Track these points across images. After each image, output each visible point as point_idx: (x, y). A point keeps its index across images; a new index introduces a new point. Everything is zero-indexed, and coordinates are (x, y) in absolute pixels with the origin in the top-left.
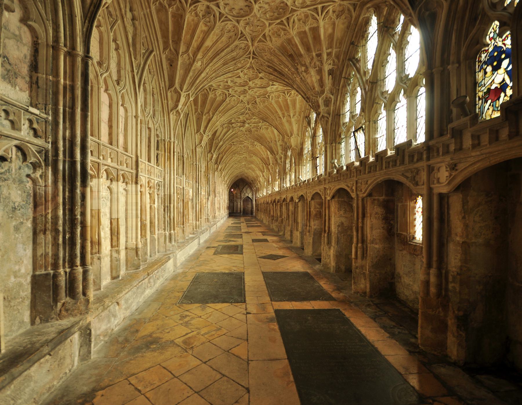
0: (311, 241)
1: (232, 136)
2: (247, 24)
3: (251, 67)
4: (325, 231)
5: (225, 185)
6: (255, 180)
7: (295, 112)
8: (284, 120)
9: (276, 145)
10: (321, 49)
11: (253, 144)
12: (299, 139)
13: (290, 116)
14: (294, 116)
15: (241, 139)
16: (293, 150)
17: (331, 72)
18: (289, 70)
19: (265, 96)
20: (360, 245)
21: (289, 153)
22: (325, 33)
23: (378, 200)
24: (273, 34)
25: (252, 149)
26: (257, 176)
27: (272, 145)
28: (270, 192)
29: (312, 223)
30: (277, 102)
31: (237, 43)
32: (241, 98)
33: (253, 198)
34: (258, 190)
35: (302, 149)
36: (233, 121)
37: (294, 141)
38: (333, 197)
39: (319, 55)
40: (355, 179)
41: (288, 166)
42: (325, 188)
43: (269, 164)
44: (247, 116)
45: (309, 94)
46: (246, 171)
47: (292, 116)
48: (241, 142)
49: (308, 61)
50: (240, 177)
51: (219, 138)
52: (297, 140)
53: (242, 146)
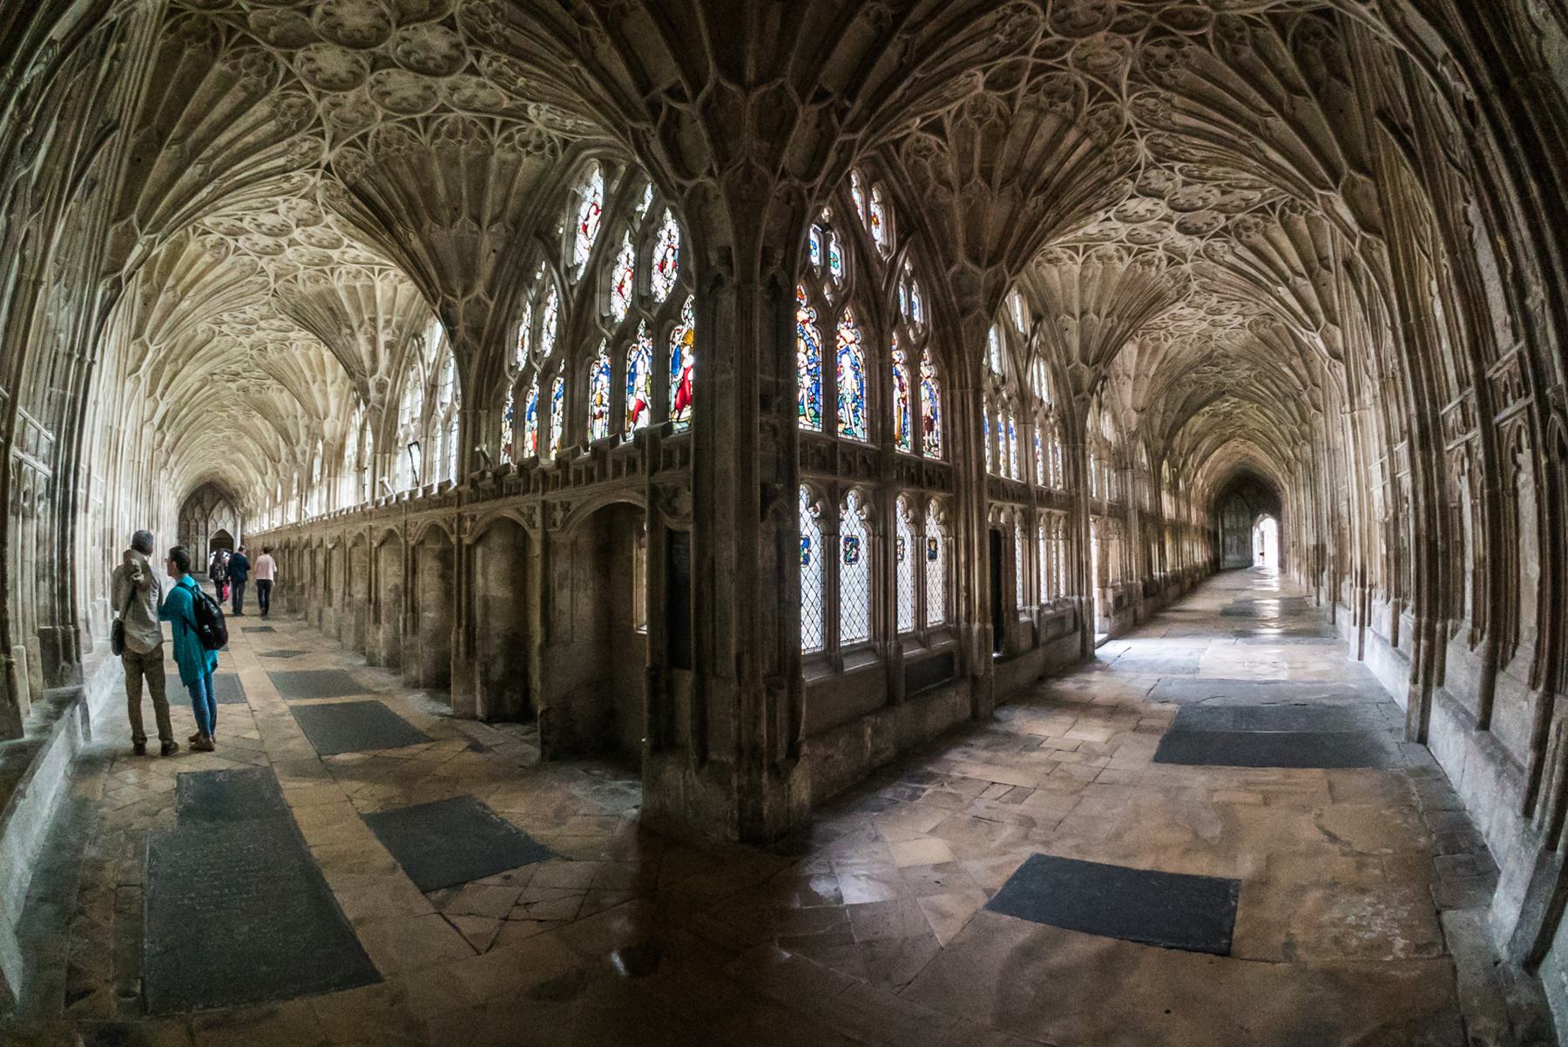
0: (353, 622)
1: (209, 397)
4: (370, 600)
5: (174, 500)
7: (336, 378)
8: (315, 388)
9: (296, 425)
12: (339, 424)
13: (325, 382)
14: (333, 382)
16: (326, 445)
18: (328, 326)
19: (284, 344)
20: (409, 614)
21: (320, 445)
22: (383, 296)
23: (432, 550)
24: (309, 278)
27: (289, 423)
28: (277, 524)
29: (354, 590)
33: (235, 534)
34: (248, 515)
35: (342, 446)
37: (328, 428)
38: (382, 544)
39: (373, 320)
40: (403, 518)
41: (316, 471)
42: (371, 527)
45: (355, 367)
46: (225, 466)
47: (329, 382)
49: (355, 325)
50: (208, 480)
52: (336, 426)
53: (224, 414)
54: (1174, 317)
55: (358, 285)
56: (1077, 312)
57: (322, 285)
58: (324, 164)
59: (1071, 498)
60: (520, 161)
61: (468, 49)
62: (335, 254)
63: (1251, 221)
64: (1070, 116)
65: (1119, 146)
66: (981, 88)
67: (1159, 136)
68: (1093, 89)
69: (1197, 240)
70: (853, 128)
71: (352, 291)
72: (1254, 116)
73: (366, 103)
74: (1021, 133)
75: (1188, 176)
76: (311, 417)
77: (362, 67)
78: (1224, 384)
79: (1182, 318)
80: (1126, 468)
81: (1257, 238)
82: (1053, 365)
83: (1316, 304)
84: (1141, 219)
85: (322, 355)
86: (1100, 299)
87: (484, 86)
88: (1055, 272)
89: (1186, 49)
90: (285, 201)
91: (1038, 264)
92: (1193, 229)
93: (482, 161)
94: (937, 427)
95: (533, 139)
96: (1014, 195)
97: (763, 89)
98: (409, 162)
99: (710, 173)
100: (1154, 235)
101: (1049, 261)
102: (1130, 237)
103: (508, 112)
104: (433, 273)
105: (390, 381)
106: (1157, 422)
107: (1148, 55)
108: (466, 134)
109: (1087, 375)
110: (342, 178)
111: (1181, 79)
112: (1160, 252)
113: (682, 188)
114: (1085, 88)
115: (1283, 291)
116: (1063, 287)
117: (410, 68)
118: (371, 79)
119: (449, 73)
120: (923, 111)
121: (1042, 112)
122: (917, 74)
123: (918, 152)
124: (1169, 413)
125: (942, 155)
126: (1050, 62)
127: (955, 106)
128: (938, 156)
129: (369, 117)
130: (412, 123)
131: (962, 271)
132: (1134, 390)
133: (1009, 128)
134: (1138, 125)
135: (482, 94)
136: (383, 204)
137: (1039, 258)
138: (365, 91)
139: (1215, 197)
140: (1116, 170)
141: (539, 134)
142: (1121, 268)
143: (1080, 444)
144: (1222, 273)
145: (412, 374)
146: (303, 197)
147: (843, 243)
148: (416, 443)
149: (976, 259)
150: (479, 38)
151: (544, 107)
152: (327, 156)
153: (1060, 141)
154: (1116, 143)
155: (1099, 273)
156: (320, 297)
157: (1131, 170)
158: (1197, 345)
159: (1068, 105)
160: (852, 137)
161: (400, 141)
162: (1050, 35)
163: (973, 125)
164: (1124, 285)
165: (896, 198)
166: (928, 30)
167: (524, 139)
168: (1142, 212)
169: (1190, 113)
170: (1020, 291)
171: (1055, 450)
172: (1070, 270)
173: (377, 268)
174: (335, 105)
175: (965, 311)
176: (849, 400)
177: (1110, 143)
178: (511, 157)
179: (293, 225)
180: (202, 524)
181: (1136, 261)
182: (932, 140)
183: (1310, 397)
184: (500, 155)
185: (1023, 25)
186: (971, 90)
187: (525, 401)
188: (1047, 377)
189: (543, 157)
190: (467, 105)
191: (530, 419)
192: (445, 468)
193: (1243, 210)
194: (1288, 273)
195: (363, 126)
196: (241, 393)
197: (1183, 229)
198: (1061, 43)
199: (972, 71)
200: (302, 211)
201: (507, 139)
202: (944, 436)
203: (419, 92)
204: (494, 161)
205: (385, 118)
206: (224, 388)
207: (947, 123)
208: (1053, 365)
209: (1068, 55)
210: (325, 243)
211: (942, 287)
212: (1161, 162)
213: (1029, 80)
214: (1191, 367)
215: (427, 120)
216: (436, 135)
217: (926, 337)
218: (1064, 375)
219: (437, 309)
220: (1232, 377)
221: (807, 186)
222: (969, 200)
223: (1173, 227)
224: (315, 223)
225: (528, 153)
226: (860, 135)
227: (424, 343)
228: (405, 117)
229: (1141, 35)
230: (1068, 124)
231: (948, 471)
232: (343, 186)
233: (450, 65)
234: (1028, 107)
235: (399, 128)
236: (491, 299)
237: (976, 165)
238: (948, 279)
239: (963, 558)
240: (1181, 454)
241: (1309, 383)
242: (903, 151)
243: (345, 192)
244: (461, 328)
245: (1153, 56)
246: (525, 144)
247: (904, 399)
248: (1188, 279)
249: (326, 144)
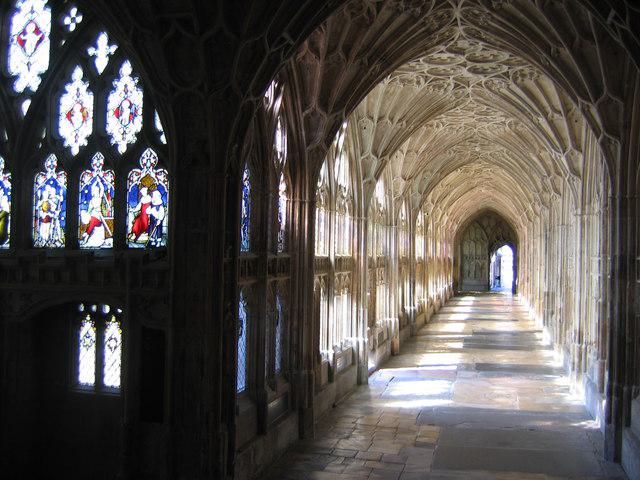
56: (376, 118)
74: (377, 24)
81: (530, 83)
82: (350, 154)
83: (566, 134)
86: (396, 109)
96: (362, 63)
112: (451, 81)
115: (542, 121)
131: (314, 113)
132: (405, 162)
140: (435, 41)
142: (417, 89)
163: (347, 14)
164: (418, 100)
183: (552, 181)
193: (523, 64)
194: (549, 109)
197: (474, 71)
208: (350, 154)
211: (296, 121)
231: (287, 260)
237: (341, 43)
238: (302, 119)
239: (295, 323)
241: (552, 171)
248: (468, 96)
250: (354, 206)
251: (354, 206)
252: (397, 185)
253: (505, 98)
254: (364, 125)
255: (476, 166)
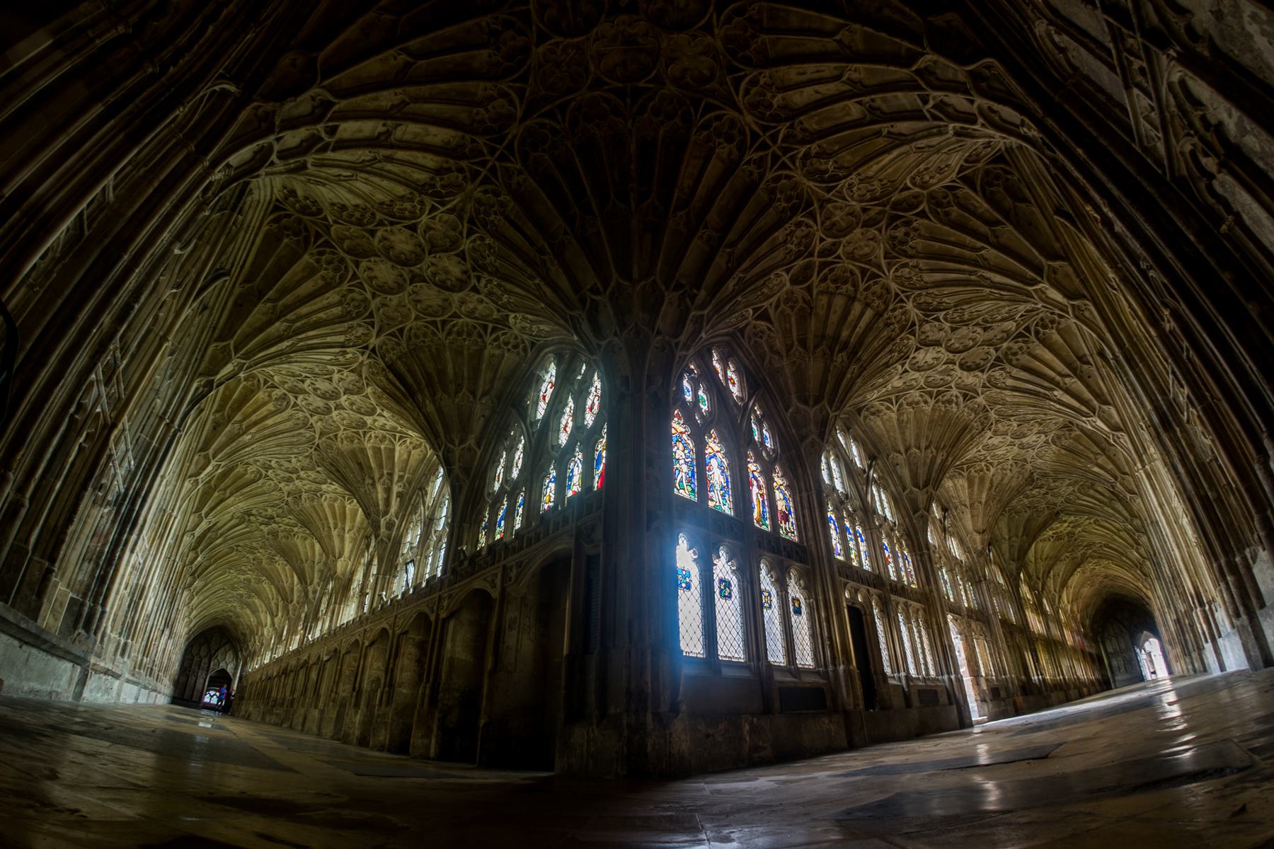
0: (334, 716)
2: (321, 420)
3: (310, 457)
6: (252, 633)
7: (353, 527)
8: (335, 533)
9: (312, 568)
10: (393, 468)
11: (271, 560)
12: (350, 564)
13: (344, 529)
15: (254, 544)
17: (400, 495)
19: (316, 494)
22: (400, 457)
24: (346, 438)
25: (267, 566)
26: (260, 623)
27: (306, 566)
30: (332, 507)
31: (302, 431)
32: (280, 486)
33: (235, 674)
35: (350, 581)
36: (254, 512)
39: (391, 475)
43: (292, 601)
44: (280, 511)
47: (347, 529)
48: (252, 550)
49: (377, 476)
50: (220, 623)
51: (220, 532)
52: (347, 565)
53: (251, 557)
54: (987, 448)
55: (382, 447)
56: (902, 450)
57: (356, 445)
58: (371, 347)
59: (926, 594)
60: (503, 356)
61: (472, 274)
62: (369, 420)
63: (1015, 347)
64: (852, 294)
65: (894, 310)
66: (788, 284)
67: (920, 295)
68: (863, 272)
69: (980, 374)
70: (702, 307)
71: (377, 451)
72: (973, 255)
73: (404, 306)
75: (952, 323)
76: (327, 556)
77: (404, 280)
78: (1055, 504)
79: (995, 447)
80: (980, 581)
82: (892, 492)
84: (931, 367)
85: (344, 507)
86: (918, 437)
87: (481, 301)
88: (879, 423)
89: (915, 224)
90: (339, 371)
91: (865, 418)
92: (973, 366)
93: (478, 354)
94: (792, 519)
95: (512, 341)
97: (643, 283)
98: (430, 351)
99: (615, 334)
100: (947, 378)
101: (873, 414)
102: (928, 384)
103: (496, 321)
104: (440, 428)
105: (397, 522)
106: (1005, 547)
107: (893, 238)
108: (469, 335)
109: (921, 497)
110: (383, 357)
111: (920, 248)
112: (955, 392)
113: (599, 346)
114: (857, 272)
116: (888, 432)
117: (436, 285)
118: (410, 288)
119: (460, 290)
120: (753, 304)
121: (832, 295)
122: (738, 274)
123: (755, 335)
124: (1014, 539)
125: (772, 335)
126: (829, 259)
127: (774, 300)
128: (769, 336)
129: (406, 317)
130: (434, 323)
131: (798, 411)
132: (973, 516)
133: (811, 308)
134: (903, 292)
135: (480, 307)
136: (410, 380)
137: (864, 413)
138: (404, 296)
139: (981, 335)
140: (897, 330)
141: (516, 338)
142: (928, 409)
143: (925, 551)
144: (1009, 396)
145: (415, 517)
146: (352, 371)
147: (707, 391)
148: (412, 561)
149: (806, 402)
150: (479, 267)
151: (520, 316)
152: (374, 342)
153: (849, 312)
154: (891, 307)
155: (912, 416)
156: (353, 452)
157: (910, 328)
158: (1015, 470)
159: (849, 286)
160: (701, 313)
161: (425, 335)
162: (824, 240)
163: (788, 311)
165: (746, 368)
166: (741, 245)
167: (506, 340)
168: (931, 361)
169: (932, 271)
170: (855, 440)
171: (905, 559)
172: (891, 417)
173: (398, 435)
174: (384, 305)
175: (803, 438)
176: (718, 488)
177: (886, 309)
178: (497, 352)
179: (342, 391)
180: (205, 660)
181: (937, 402)
182: (763, 324)
184: (489, 350)
185: (806, 236)
186: (783, 287)
187: (497, 515)
188: (888, 502)
189: (518, 354)
190: (470, 314)
191: (499, 526)
192: (434, 568)
195: (401, 322)
196: (270, 537)
198: (834, 244)
199: (778, 271)
200: (350, 383)
201: (496, 339)
202: (798, 526)
203: (440, 303)
204: (486, 353)
205: (417, 318)
206: (258, 529)
207: (771, 311)
208: (892, 492)
209: (840, 251)
210: (363, 410)
212: (928, 316)
213: (818, 275)
214: (1019, 491)
215: (444, 323)
216: (449, 334)
217: (776, 458)
218: (902, 499)
219: (441, 455)
220: (1060, 495)
221: (674, 341)
222: (795, 362)
223: (957, 367)
224: (358, 393)
225: (509, 350)
226: (706, 312)
227: (426, 494)
228: (429, 319)
229: (883, 223)
230: (852, 299)
232: (383, 365)
233: (460, 285)
234: (822, 293)
235: (426, 327)
236: (479, 448)
237: (795, 338)
239: (823, 615)
240: (1038, 578)
242: (746, 335)
243: (384, 370)
244: (456, 467)
245: (896, 237)
246: (507, 344)
247: (762, 495)
249: (374, 332)
250: (912, 542)
251: (912, 542)
252: (974, 541)
253: (1015, 389)
254: (895, 462)
255: (1062, 527)
